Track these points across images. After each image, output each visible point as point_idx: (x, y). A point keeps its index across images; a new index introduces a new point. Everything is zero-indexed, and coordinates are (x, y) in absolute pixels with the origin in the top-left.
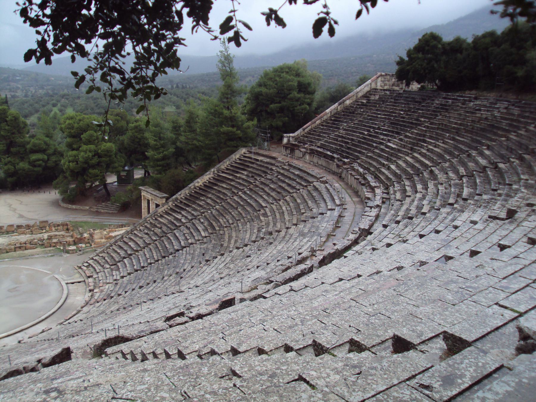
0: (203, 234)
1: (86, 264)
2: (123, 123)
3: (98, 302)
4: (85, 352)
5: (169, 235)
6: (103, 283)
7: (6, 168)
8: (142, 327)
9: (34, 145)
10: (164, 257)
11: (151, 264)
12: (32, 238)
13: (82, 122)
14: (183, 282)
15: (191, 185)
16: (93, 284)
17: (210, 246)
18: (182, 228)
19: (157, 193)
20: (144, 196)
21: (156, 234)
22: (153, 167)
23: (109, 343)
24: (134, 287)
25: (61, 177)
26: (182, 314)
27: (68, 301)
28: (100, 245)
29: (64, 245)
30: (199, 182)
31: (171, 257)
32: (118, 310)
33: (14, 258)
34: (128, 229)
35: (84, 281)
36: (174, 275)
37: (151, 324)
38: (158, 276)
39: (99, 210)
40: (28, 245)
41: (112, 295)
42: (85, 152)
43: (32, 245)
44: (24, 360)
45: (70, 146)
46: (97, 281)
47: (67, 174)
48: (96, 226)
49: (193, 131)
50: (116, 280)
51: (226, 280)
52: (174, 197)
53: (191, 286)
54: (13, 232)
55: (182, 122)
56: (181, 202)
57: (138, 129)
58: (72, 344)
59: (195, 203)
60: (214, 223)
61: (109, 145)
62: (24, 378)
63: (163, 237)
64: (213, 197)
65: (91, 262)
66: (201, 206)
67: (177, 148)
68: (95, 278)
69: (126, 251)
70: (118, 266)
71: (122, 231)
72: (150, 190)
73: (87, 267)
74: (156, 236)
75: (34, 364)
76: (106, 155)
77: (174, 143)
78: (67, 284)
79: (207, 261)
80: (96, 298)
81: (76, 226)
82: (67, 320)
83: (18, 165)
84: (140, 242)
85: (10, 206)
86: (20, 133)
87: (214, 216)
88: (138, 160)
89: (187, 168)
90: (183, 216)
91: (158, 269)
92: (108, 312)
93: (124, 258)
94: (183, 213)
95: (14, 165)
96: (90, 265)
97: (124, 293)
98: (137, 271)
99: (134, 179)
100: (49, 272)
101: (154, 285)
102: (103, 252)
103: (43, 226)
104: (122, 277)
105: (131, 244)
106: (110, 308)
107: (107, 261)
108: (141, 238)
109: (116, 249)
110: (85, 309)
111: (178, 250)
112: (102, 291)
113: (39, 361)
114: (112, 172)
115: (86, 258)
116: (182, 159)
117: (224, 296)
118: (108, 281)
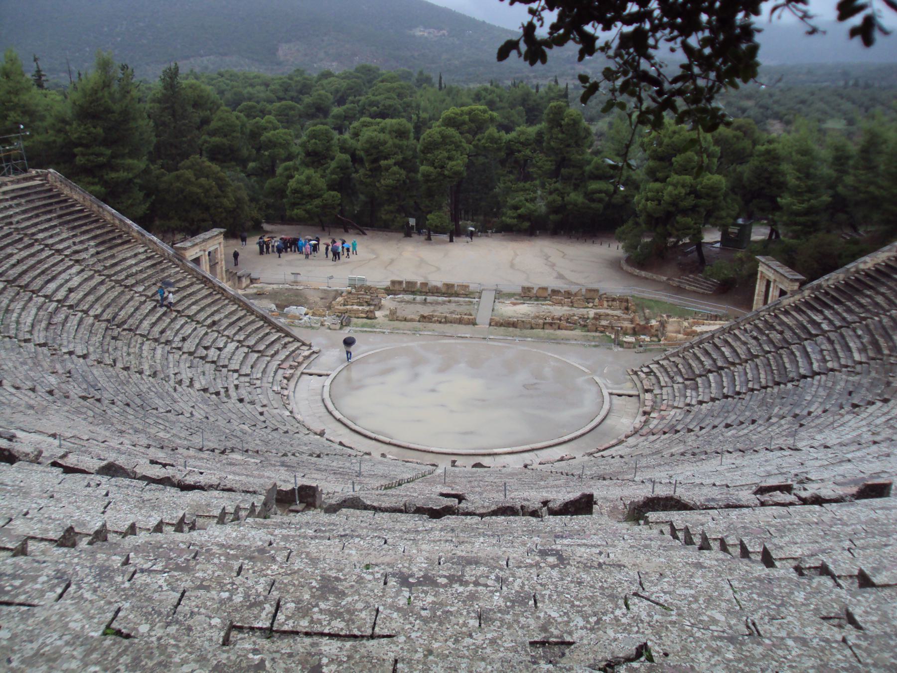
0: (857, 357)
1: (646, 370)
2: (746, 143)
3: (653, 434)
4: (615, 508)
5: (793, 348)
7: (550, 198)
8: (715, 493)
9: (597, 168)
10: (778, 384)
11: (752, 390)
12: (571, 313)
13: (677, 136)
14: (803, 433)
15: (851, 266)
16: (651, 403)
17: (866, 381)
18: (820, 339)
19: (785, 270)
20: (762, 272)
21: (771, 341)
22: (786, 224)
23: (654, 504)
24: (716, 423)
25: (630, 223)
26: (787, 489)
27: (608, 422)
28: (673, 343)
29: (617, 333)
30: (867, 262)
31: (790, 385)
32: (683, 454)
33: (539, 338)
34: (725, 324)
35: (639, 396)
36: (789, 418)
37: (732, 491)
38: (761, 413)
39: (682, 286)
40: (563, 323)
41: (678, 428)
42: (675, 186)
43: (569, 323)
44: (526, 495)
45: (652, 174)
46: (658, 400)
47: (641, 220)
48: (672, 311)
49: (871, 168)
50: (689, 405)
51: (884, 448)
52: (815, 282)
53: (816, 444)
54: (545, 299)
55: (853, 148)
56: (827, 293)
57: (773, 157)
58: (598, 491)
59: (851, 299)
60: (881, 341)
61: (717, 178)
62: (519, 521)
63: (782, 348)
64: (888, 292)
65: (654, 367)
66: (861, 306)
67: (836, 196)
68: (656, 395)
69: (714, 361)
70: (697, 383)
71: (714, 326)
72: (775, 264)
73: (647, 374)
74: (771, 346)
75: (538, 505)
76: (708, 195)
77: (832, 186)
78: (611, 394)
79: (855, 406)
80: (651, 426)
81: (641, 304)
82: (600, 451)
83: (568, 195)
84: (742, 350)
85: (547, 258)
86: (578, 145)
87: (884, 328)
88: (762, 210)
89: (848, 234)
90: (826, 318)
91: (763, 403)
92: (666, 453)
93: (710, 371)
94: (827, 312)
95: (562, 195)
96: (652, 371)
97: (698, 428)
98: (726, 397)
99: (749, 242)
100: (586, 371)
101: (751, 427)
102: (677, 355)
103: (591, 296)
104: (701, 403)
105: (726, 351)
106: (671, 448)
107: (680, 372)
108: (745, 343)
109: (699, 355)
110: (631, 441)
111: (805, 377)
112: (663, 418)
113: (545, 503)
114: (714, 225)
115: (647, 359)
116: (842, 216)
117: (871, 477)
118: (676, 404)
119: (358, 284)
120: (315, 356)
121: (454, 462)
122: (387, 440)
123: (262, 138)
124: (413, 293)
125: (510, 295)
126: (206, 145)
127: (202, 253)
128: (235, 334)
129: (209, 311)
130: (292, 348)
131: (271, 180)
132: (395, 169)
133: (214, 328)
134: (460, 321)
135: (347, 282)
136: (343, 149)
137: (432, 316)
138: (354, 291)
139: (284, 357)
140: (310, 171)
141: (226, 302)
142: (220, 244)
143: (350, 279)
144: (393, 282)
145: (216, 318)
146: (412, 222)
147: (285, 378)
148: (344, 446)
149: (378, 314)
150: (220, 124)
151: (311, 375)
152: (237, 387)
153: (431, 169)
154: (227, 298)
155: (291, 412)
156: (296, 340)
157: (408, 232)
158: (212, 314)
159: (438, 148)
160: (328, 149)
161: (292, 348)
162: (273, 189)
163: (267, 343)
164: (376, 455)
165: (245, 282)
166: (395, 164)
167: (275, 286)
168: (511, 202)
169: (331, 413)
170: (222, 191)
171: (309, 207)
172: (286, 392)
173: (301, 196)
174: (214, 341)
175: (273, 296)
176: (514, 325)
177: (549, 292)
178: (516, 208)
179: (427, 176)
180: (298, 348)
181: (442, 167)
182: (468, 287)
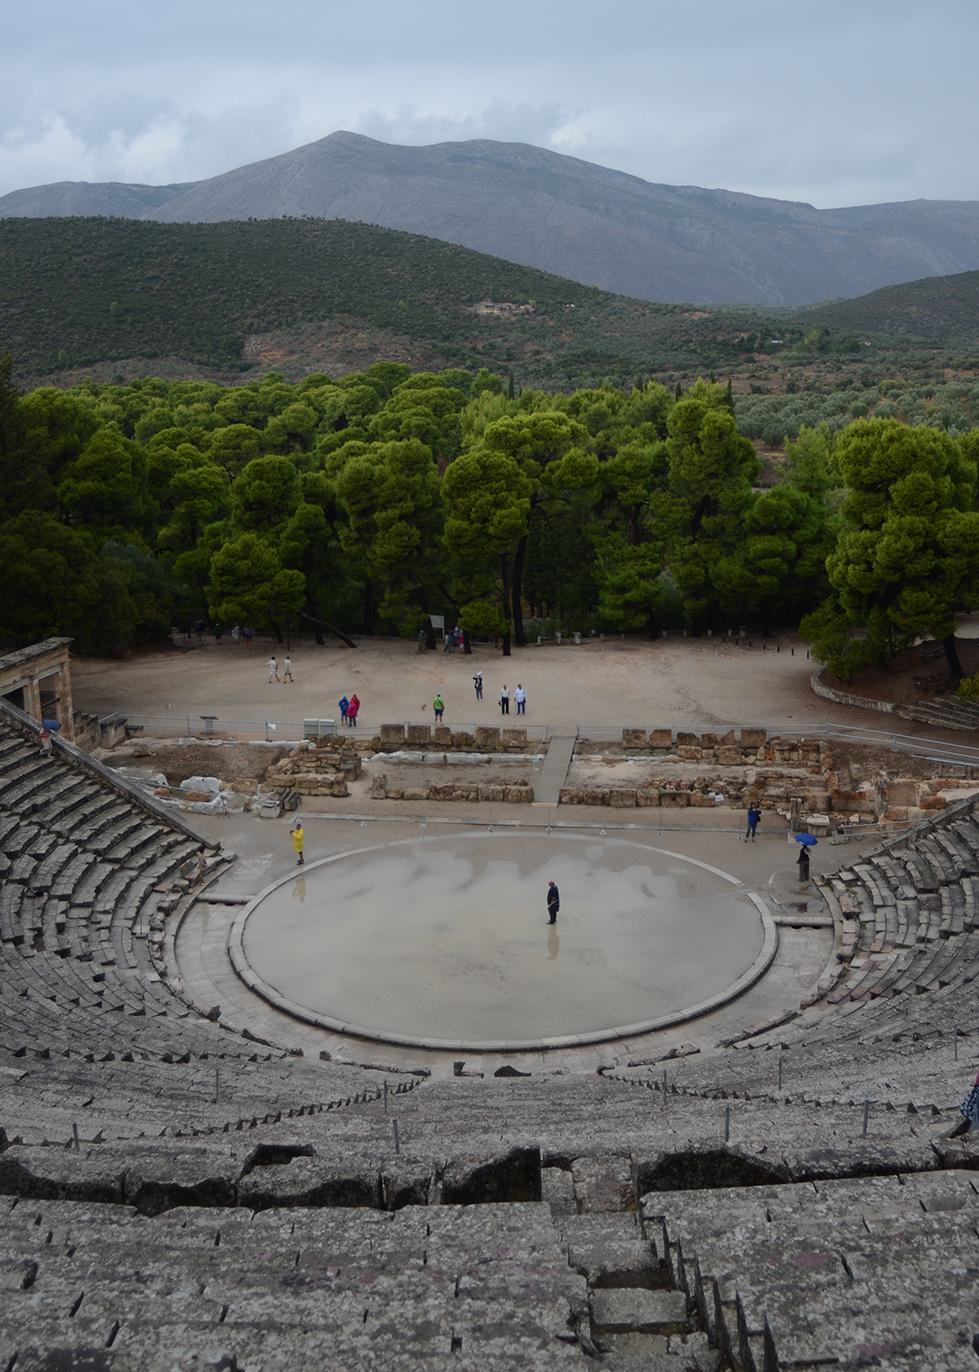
3: (853, 1000)
6: (885, 943)
12: (713, 775)
13: (896, 445)
16: (853, 940)
24: (970, 974)
27: (772, 977)
32: (896, 1039)
35: (832, 926)
39: (924, 718)
41: (900, 985)
46: (868, 933)
50: (922, 940)
65: (862, 870)
70: (940, 898)
73: (849, 883)
78: (779, 925)
80: (851, 984)
82: (749, 1036)
83: (716, 563)
93: (966, 874)
96: (858, 878)
97: (936, 985)
100: (735, 881)
102: (904, 844)
106: (879, 1026)
107: (911, 876)
109: (946, 844)
118: (899, 940)
119: (321, 733)
120: (226, 866)
121: (459, 1067)
122: (339, 1025)
123: (172, 482)
124: (423, 747)
125: (603, 746)
126: (70, 495)
127: (26, 682)
128: (72, 830)
129: (28, 787)
130: (181, 852)
131: (186, 554)
132: (400, 526)
133: (34, 819)
134: (504, 797)
135: (301, 731)
136: (312, 496)
137: (453, 789)
138: (312, 746)
139: (163, 870)
140: (249, 536)
141: (63, 770)
142: (62, 665)
143: (307, 725)
144: (386, 729)
145: (40, 800)
146: (438, 622)
147: (160, 909)
148: (252, 1038)
149: (354, 787)
150: (94, 458)
151: (213, 902)
152: (61, 928)
153: (465, 525)
154: (65, 764)
155: (163, 975)
156: (191, 838)
157: (430, 642)
158: (34, 792)
159: (476, 487)
160: (285, 495)
161: (181, 852)
162: (189, 569)
163: (134, 844)
164: (312, 1054)
165: (114, 734)
166: (401, 517)
167: (168, 742)
168: (613, 579)
169: (239, 975)
170: (79, 573)
171: (247, 598)
172: (157, 937)
173: (238, 579)
174: (31, 842)
175: (161, 759)
176: (604, 800)
177: (675, 738)
178: (622, 589)
179: (458, 536)
180: (193, 854)
181: (485, 520)
182: (524, 732)
